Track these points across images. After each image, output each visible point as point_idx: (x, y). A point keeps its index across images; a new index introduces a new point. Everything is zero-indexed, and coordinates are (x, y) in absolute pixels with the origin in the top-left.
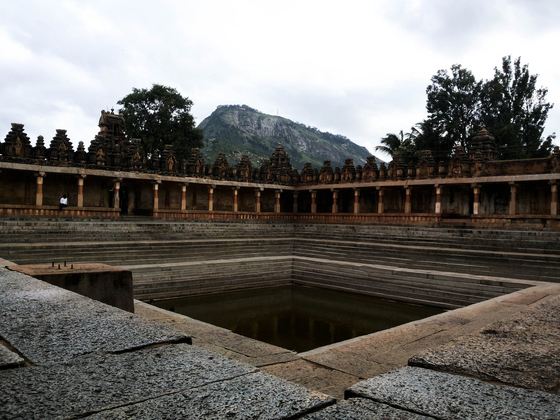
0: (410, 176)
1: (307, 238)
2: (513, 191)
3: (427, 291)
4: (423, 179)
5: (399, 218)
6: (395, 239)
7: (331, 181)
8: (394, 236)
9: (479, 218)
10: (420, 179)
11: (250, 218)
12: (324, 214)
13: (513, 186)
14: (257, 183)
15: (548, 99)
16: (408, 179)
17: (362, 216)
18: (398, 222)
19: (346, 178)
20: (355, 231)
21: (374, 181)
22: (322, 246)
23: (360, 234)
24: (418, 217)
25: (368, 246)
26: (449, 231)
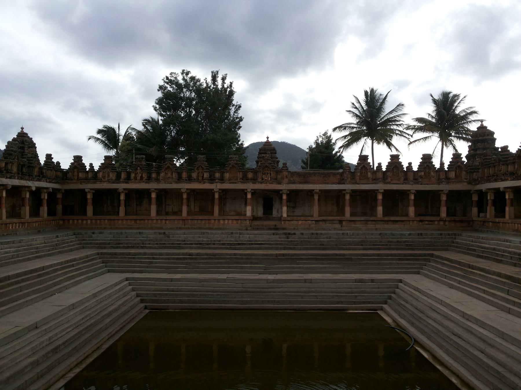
0: (219, 180)
1: (105, 248)
2: (316, 197)
3: (316, 296)
4: (233, 183)
5: (207, 221)
6: (223, 244)
7: (116, 179)
8: (220, 241)
9: (288, 220)
10: (230, 183)
11: (19, 227)
12: (108, 217)
13: (316, 193)
14: (26, 180)
15: (241, 113)
16: (217, 182)
17: (161, 220)
18: (207, 226)
19: (138, 178)
20: (169, 237)
21: (177, 183)
22: (149, 258)
23: (178, 241)
24: (228, 220)
25: (207, 254)
26: (274, 234)
